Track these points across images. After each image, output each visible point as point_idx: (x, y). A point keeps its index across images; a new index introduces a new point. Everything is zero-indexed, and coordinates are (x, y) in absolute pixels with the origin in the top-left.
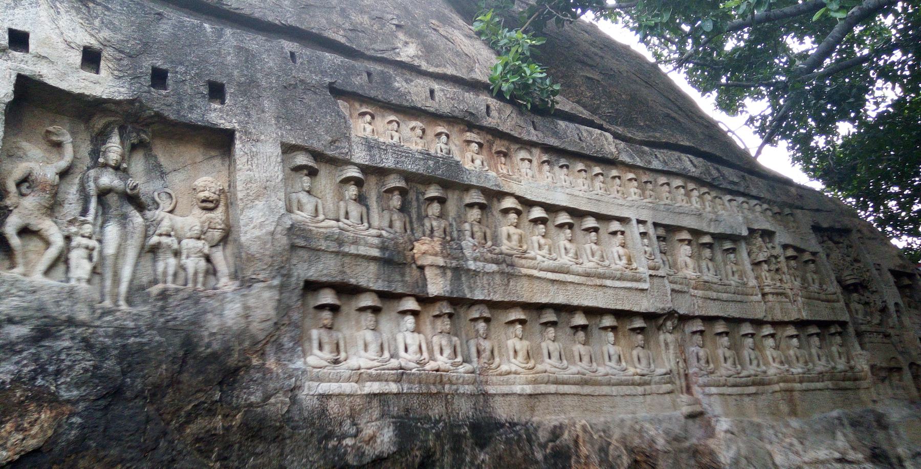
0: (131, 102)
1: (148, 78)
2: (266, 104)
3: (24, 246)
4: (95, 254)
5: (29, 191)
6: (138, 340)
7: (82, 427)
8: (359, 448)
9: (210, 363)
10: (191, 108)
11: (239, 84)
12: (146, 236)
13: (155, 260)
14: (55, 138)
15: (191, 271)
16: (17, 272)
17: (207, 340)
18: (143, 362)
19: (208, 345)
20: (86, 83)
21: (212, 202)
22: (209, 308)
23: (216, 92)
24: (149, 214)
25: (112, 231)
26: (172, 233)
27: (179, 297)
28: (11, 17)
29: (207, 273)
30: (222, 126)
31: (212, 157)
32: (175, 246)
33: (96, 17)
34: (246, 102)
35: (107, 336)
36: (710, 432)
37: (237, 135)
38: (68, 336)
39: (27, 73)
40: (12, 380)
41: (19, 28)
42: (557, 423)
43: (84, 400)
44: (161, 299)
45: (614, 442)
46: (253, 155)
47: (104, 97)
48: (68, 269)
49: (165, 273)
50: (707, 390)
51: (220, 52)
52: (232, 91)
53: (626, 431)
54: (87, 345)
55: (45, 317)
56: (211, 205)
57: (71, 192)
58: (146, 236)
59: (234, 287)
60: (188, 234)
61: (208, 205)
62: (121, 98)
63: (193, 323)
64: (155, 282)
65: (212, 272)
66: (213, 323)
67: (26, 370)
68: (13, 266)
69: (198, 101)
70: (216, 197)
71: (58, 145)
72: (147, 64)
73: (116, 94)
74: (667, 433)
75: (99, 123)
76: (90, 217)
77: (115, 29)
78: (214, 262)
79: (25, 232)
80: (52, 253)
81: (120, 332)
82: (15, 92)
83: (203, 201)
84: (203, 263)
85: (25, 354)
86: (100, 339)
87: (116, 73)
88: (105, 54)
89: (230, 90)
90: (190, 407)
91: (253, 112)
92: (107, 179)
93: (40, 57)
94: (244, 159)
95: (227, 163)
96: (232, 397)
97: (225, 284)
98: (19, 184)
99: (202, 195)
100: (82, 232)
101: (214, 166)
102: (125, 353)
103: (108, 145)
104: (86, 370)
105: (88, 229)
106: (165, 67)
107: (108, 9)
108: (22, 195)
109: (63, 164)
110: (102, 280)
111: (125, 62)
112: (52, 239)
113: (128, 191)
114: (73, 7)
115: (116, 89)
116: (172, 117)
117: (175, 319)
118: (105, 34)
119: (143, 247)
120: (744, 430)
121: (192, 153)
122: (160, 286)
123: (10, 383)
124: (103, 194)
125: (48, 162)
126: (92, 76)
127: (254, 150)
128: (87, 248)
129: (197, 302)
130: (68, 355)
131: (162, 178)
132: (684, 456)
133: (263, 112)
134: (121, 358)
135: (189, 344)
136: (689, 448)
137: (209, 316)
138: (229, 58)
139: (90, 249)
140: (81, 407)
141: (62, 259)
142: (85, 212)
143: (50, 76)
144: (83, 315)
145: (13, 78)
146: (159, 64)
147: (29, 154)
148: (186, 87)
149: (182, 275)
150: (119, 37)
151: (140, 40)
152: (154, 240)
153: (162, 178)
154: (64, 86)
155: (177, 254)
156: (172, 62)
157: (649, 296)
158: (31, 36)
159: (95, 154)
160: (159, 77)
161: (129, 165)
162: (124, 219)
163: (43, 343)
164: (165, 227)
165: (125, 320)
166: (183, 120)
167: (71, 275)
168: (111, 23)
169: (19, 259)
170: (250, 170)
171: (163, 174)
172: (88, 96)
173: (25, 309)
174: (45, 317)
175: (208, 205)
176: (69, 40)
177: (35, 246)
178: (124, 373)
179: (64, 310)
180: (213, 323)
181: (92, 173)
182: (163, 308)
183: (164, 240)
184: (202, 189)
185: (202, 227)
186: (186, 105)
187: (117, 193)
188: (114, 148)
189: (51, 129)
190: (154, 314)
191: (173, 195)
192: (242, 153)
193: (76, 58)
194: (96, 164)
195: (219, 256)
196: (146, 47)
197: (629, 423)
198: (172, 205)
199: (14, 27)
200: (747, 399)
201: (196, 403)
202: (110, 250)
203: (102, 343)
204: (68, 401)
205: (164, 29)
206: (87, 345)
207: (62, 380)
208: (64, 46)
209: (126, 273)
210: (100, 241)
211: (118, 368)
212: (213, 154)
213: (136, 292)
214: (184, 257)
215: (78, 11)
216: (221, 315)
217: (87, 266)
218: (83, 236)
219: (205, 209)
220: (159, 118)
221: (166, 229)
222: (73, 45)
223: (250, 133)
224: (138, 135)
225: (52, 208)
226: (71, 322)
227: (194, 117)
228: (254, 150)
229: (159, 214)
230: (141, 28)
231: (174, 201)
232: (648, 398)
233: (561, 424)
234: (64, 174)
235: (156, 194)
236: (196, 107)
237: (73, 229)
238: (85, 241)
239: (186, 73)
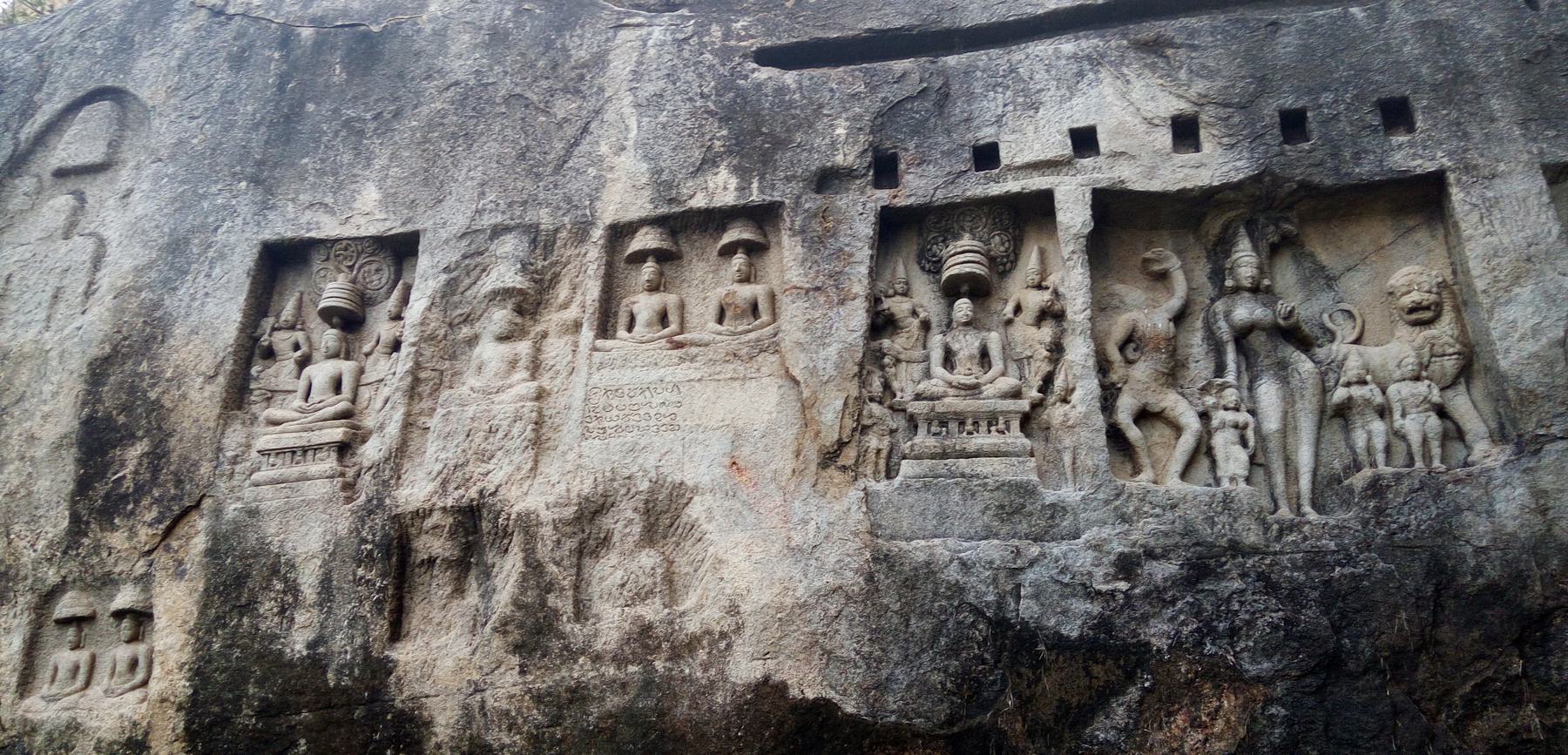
0: (1256, 179)
1: (1277, 131)
2: (1495, 104)
3: (1146, 437)
4: (1250, 434)
5: (1138, 354)
6: (1348, 570)
7: (1288, 721)
10: (1357, 158)
11: (1435, 88)
12: (1325, 391)
13: (1347, 429)
14: (1156, 268)
15: (1415, 439)
16: (1145, 476)
17: (1472, 563)
18: (1365, 608)
19: (1478, 571)
20: (1186, 171)
21: (1428, 308)
22: (1464, 503)
23: (1396, 114)
24: (1321, 353)
25: (1268, 393)
26: (1369, 378)
27: (1405, 486)
28: (1069, 113)
29: (1445, 438)
30: (1419, 171)
31: (1411, 230)
32: (1379, 399)
33: (1180, 68)
34: (1454, 114)
35: (1295, 567)
37: (1452, 177)
38: (1234, 573)
39: (1104, 184)
40: (1170, 646)
41: (1081, 124)
43: (1283, 678)
44: (1373, 496)
46: (1491, 205)
47: (1216, 183)
48: (1214, 463)
49: (1369, 450)
51: (1387, 44)
52: (1425, 103)
54: (1268, 585)
55: (1197, 544)
56: (1427, 315)
57: (1195, 344)
58: (1325, 391)
59: (1503, 458)
60: (1397, 374)
61: (1422, 316)
62: (1241, 176)
63: (1440, 533)
64: (1357, 467)
65: (1454, 433)
66: (1478, 529)
67: (1186, 630)
68: (1137, 471)
69: (1367, 141)
70: (1433, 297)
71: (1163, 277)
72: (1270, 109)
73: (1232, 174)
75: (1214, 227)
76: (1230, 377)
77: (1211, 75)
78: (1456, 416)
79: (1144, 416)
80: (1187, 441)
81: (1316, 559)
82: (1094, 216)
83: (1412, 311)
84: (1434, 421)
85: (1179, 604)
86: (1287, 573)
87: (1225, 140)
88: (1204, 117)
89: (1419, 104)
90: (1468, 688)
91: (1473, 129)
92: (1245, 311)
93: (1116, 155)
94: (1475, 217)
95: (1440, 233)
96: (1549, 668)
97: (1485, 452)
98: (1122, 349)
99: (1407, 301)
100: (1223, 402)
101: (1417, 243)
102: (1331, 595)
103: (1235, 256)
104: (1275, 627)
105: (1230, 396)
106: (1299, 104)
107: (1194, 48)
108: (1130, 362)
109: (1175, 303)
110: (1269, 474)
111: (1236, 120)
112: (1183, 420)
113: (1281, 322)
114: (1146, 65)
115: (1230, 165)
116: (1328, 182)
117: (1405, 527)
118: (1200, 86)
119: (1322, 412)
121: (1371, 232)
122: (1367, 472)
123: (1169, 652)
124: (1242, 335)
125: (1155, 305)
126: (1190, 157)
127: (1490, 194)
128: (1236, 426)
129: (1438, 494)
130: (1242, 603)
131: (1330, 287)
133: (1492, 120)
134: (1326, 603)
135: (1441, 572)
137: (1468, 517)
138: (1407, 49)
139: (1240, 428)
140: (1280, 689)
141: (1203, 450)
142: (1220, 370)
143: (1134, 177)
144: (1252, 537)
145: (1088, 196)
146: (1289, 102)
147: (1128, 300)
148: (1341, 125)
149: (1399, 447)
150: (1220, 83)
151: (1252, 76)
152: (1340, 394)
153: (1330, 287)
154: (1155, 186)
155: (1383, 412)
156: (1310, 91)
158: (1099, 129)
159: (1218, 275)
160: (1293, 124)
161: (1272, 279)
162: (1282, 370)
163: (1200, 587)
164: (1353, 368)
165: (1319, 539)
166: (1347, 181)
167: (1220, 473)
168: (1204, 66)
169: (1144, 460)
170: (1489, 233)
171: (1330, 281)
172: (1192, 190)
173: (1166, 534)
174: (1197, 544)
175: (1422, 316)
176: (1150, 115)
177: (1162, 436)
178: (1337, 629)
179: (1219, 531)
180: (1478, 529)
181: (1220, 306)
182: (1379, 511)
183: (1356, 391)
184: (1404, 289)
185: (1419, 356)
186: (1347, 155)
187: (1263, 329)
188: (1245, 259)
189: (1148, 255)
190: (1365, 523)
191: (1355, 312)
192: (1467, 207)
193: (1165, 138)
194: (1222, 292)
195: (1460, 404)
196: (1264, 84)
198: (1357, 330)
199: (1075, 126)
201: (1478, 680)
202: (1272, 424)
203: (1291, 580)
204: (1258, 679)
205: (1287, 44)
206: (1268, 585)
207: (1242, 645)
208: (1145, 127)
209: (1304, 457)
210: (1253, 412)
211: (1325, 621)
212: (1411, 223)
213: (1327, 488)
214: (1397, 416)
215: (1153, 67)
216: (1490, 513)
217: (1242, 456)
218: (1226, 409)
219: (1415, 324)
220: (1308, 189)
221: (1355, 372)
222: (1156, 121)
223: (1476, 167)
224: (1278, 227)
225: (1173, 375)
226: (1235, 548)
227: (1365, 170)
228: (1490, 194)
229: (1338, 348)
230: (1249, 58)
231: (1359, 321)
234: (1179, 318)
235: (1325, 316)
236: (1366, 152)
237: (1210, 400)
238: (1230, 416)
239: (1336, 101)
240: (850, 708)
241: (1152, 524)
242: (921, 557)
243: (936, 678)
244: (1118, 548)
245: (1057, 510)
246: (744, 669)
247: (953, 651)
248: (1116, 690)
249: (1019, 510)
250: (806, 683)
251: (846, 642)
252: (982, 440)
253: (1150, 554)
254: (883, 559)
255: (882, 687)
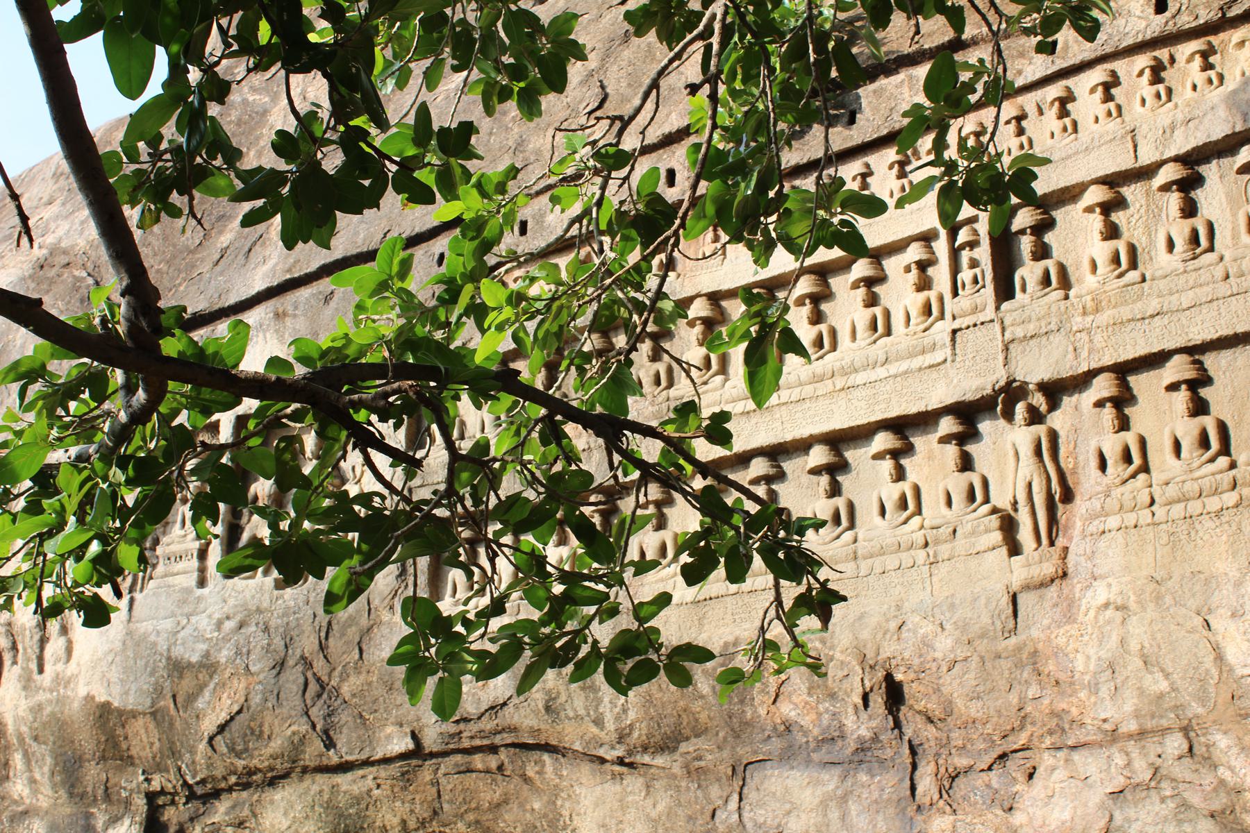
8: (474, 695)
9: (350, 626)
36: (1069, 616)
42: (731, 639)
45: (838, 655)
50: (1095, 526)
53: (865, 635)
74: (963, 626)
120: (1158, 599)
132: (1005, 664)
136: (1019, 649)
140: (261, 677)
157: (952, 372)
197: (873, 621)
200: (1208, 524)
206: (266, 629)
232: (943, 569)
233: (737, 639)
240: (116, 704)
241: (232, 602)
242: (142, 630)
243: (145, 687)
244: (217, 616)
245: (199, 599)
246: (82, 691)
247: (152, 674)
248: (205, 685)
249: (185, 602)
250: (102, 698)
251: (114, 675)
252: (181, 566)
253: (228, 618)
254: (129, 633)
255: (127, 693)
